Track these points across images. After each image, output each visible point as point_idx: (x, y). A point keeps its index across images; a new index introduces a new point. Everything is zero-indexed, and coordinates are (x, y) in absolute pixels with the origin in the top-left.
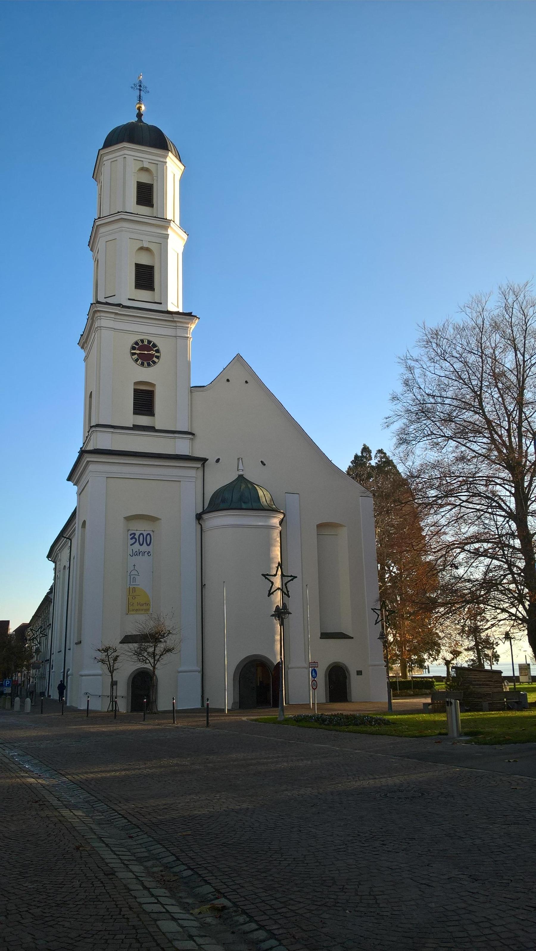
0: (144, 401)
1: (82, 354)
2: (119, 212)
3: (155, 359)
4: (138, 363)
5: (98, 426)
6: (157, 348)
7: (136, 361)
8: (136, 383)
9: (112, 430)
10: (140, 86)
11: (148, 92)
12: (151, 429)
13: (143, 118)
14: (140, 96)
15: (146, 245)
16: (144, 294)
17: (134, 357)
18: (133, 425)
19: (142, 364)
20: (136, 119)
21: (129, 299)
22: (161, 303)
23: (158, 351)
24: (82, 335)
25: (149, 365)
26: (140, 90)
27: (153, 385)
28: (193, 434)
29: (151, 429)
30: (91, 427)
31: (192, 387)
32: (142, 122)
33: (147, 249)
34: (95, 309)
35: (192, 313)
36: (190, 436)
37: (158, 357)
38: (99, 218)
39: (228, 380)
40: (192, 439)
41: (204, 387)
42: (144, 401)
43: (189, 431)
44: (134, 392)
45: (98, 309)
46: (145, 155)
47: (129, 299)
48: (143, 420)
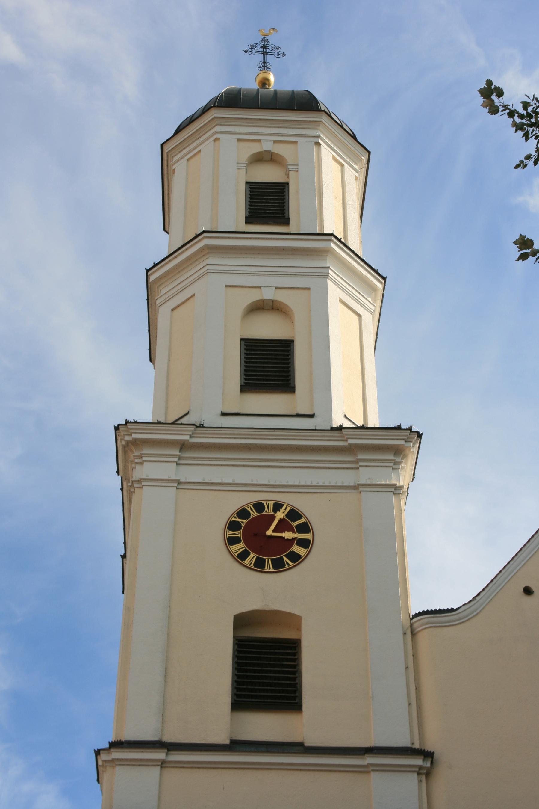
0: (266, 668)
3: (296, 549)
4: (247, 562)
6: (302, 521)
7: (243, 556)
9: (160, 755)
10: (264, 47)
11: (283, 54)
14: (265, 62)
15: (268, 295)
17: (234, 548)
19: (259, 565)
21: (224, 414)
22: (312, 416)
23: (305, 528)
25: (279, 565)
26: (265, 53)
27: (294, 621)
28: (428, 755)
31: (417, 615)
36: (418, 761)
37: (305, 544)
39: (528, 591)
40: (426, 774)
41: (452, 610)
42: (266, 668)
43: (417, 746)
46: (267, 132)
47: (224, 414)
48: (264, 725)
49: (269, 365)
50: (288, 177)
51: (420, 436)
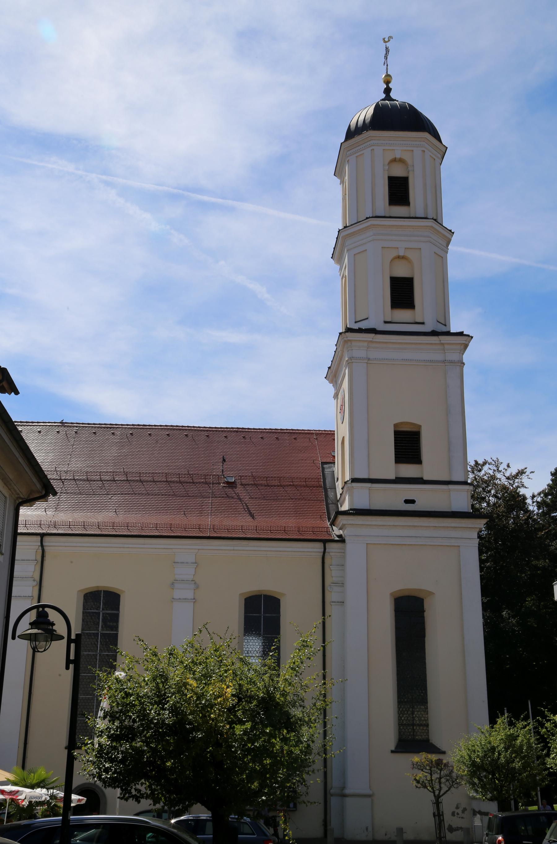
1: (330, 389)
2: (367, 218)
5: (354, 480)
8: (395, 425)
12: (419, 481)
13: (392, 95)
15: (401, 253)
16: (403, 315)
18: (396, 478)
20: (384, 96)
21: (386, 322)
22: (423, 323)
24: (329, 368)
29: (419, 481)
30: (345, 483)
32: (391, 99)
33: (404, 257)
34: (345, 339)
35: (463, 332)
38: (345, 227)
44: (395, 435)
45: (349, 338)
49: (402, 292)
50: (408, 172)
51: (472, 337)
